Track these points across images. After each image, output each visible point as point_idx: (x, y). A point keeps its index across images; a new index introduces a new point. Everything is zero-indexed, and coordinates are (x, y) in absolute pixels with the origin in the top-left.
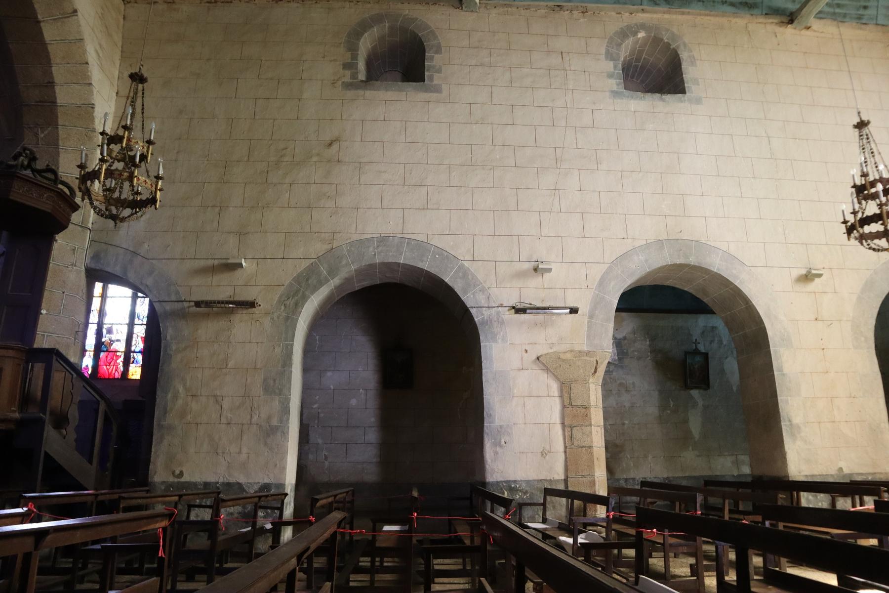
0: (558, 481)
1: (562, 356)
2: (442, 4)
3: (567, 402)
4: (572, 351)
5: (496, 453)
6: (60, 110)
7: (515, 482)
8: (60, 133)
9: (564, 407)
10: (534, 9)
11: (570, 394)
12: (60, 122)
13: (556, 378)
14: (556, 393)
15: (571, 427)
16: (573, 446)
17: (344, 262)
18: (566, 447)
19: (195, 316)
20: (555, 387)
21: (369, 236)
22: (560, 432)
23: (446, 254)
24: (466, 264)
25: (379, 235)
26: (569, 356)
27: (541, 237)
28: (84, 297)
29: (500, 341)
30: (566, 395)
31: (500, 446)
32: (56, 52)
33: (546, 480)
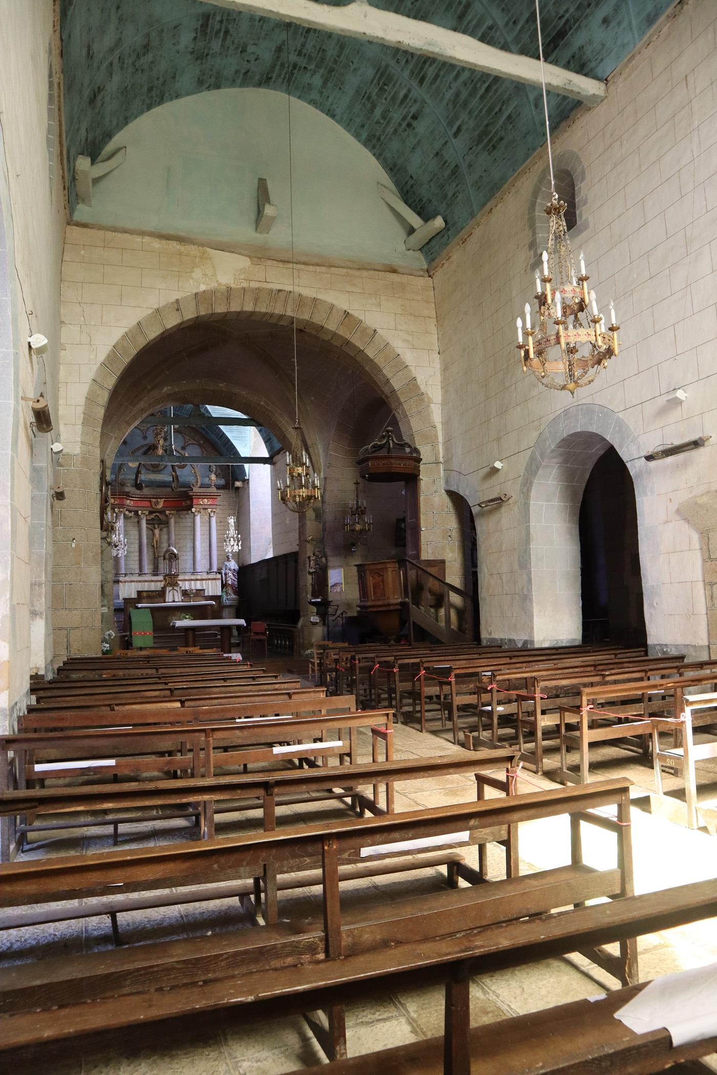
0: (702, 647)
1: (700, 501)
2: (579, 116)
3: (706, 556)
4: (708, 492)
5: (651, 615)
6: (398, 393)
7: (666, 645)
8: (405, 407)
9: (704, 561)
10: (656, 37)
11: (708, 545)
12: (402, 400)
13: (695, 527)
14: (698, 547)
15: (711, 585)
16: (713, 608)
17: (547, 444)
18: (707, 610)
19: (491, 512)
20: (695, 537)
21: (558, 413)
22: (702, 591)
23: (606, 410)
24: (621, 415)
25: (563, 410)
26: (705, 499)
27: (676, 358)
28: (451, 510)
29: (649, 493)
30: (705, 547)
31: (654, 607)
32: (379, 361)
33: (692, 646)
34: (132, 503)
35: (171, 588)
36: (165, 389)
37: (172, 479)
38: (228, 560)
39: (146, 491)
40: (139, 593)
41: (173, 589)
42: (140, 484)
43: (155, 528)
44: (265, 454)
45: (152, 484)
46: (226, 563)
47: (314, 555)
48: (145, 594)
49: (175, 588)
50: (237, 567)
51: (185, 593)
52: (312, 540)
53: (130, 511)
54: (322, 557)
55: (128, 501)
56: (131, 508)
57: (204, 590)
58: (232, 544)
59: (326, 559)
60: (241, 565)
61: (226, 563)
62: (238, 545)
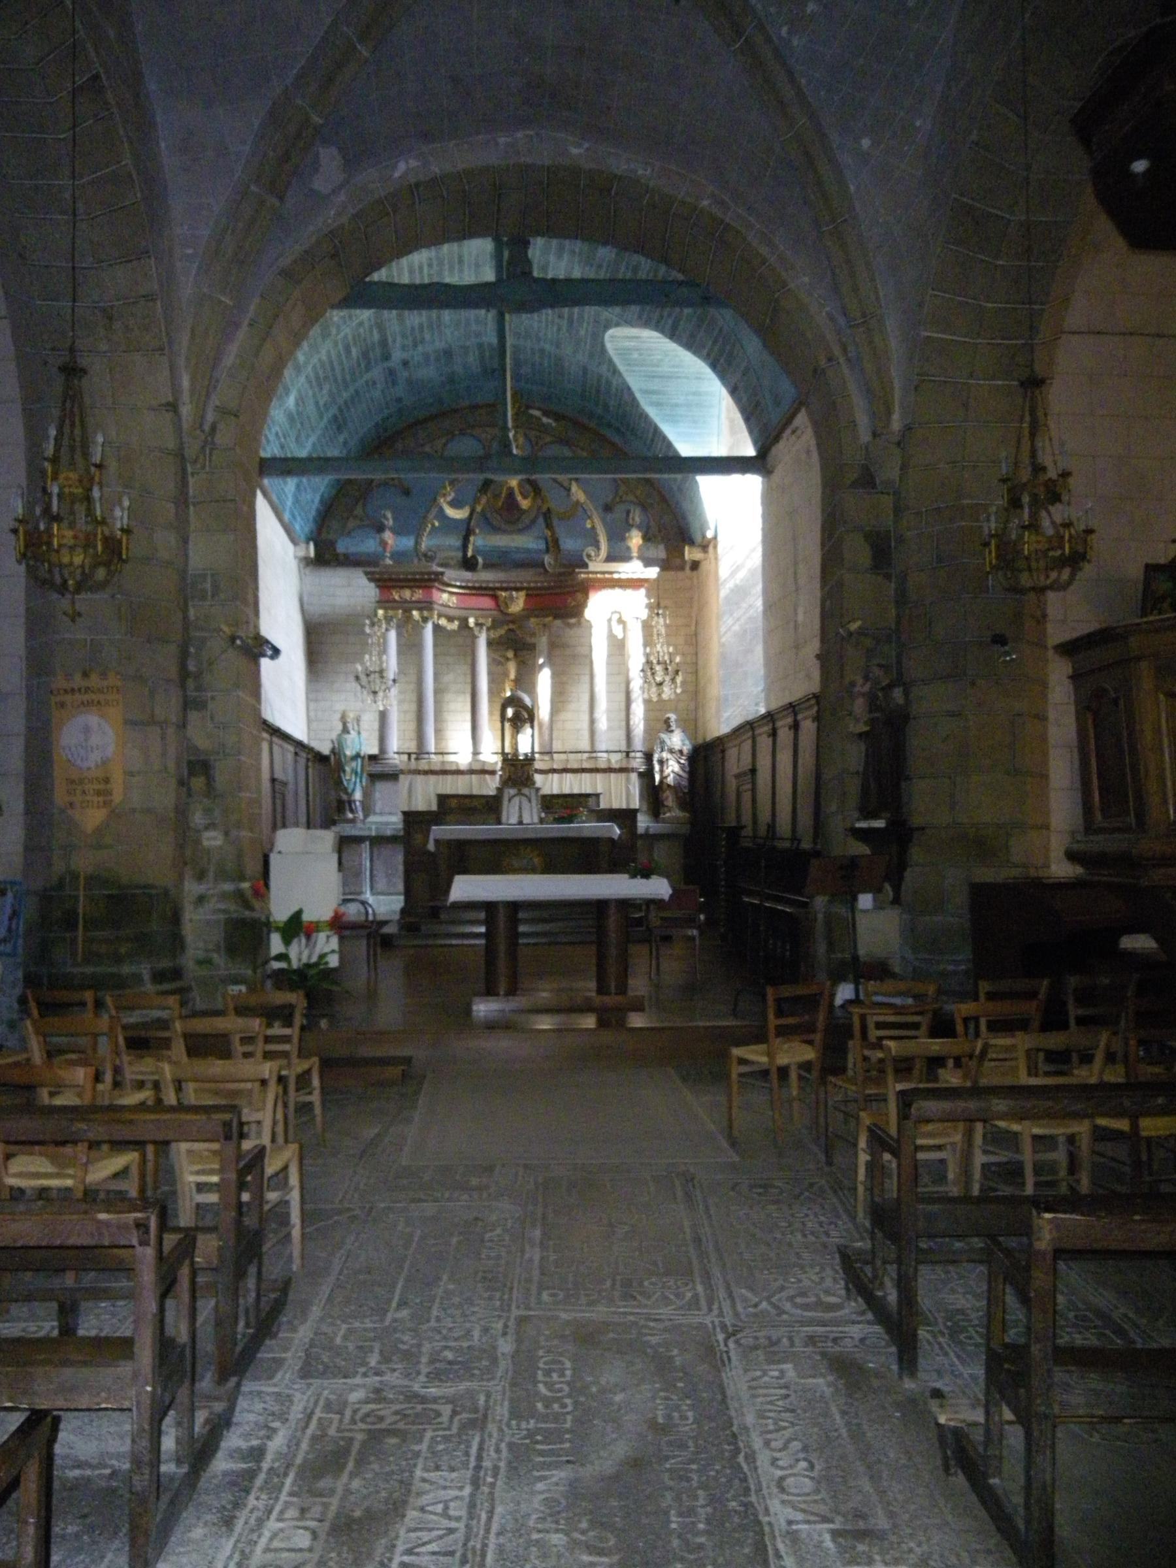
34: (454, 599)
35: (512, 791)
36: (402, 167)
37: (542, 546)
38: (669, 730)
39: (486, 577)
40: (442, 799)
41: (520, 793)
42: (474, 557)
43: (508, 659)
44: (749, 450)
45: (500, 560)
46: (663, 736)
47: (866, 678)
48: (454, 803)
49: (526, 791)
50: (687, 748)
51: (550, 803)
52: (861, 632)
53: (450, 619)
54: (890, 686)
55: (445, 596)
56: (452, 613)
57: (597, 796)
58: (658, 679)
59: (906, 694)
60: (700, 741)
61: (663, 736)
62: (673, 680)
